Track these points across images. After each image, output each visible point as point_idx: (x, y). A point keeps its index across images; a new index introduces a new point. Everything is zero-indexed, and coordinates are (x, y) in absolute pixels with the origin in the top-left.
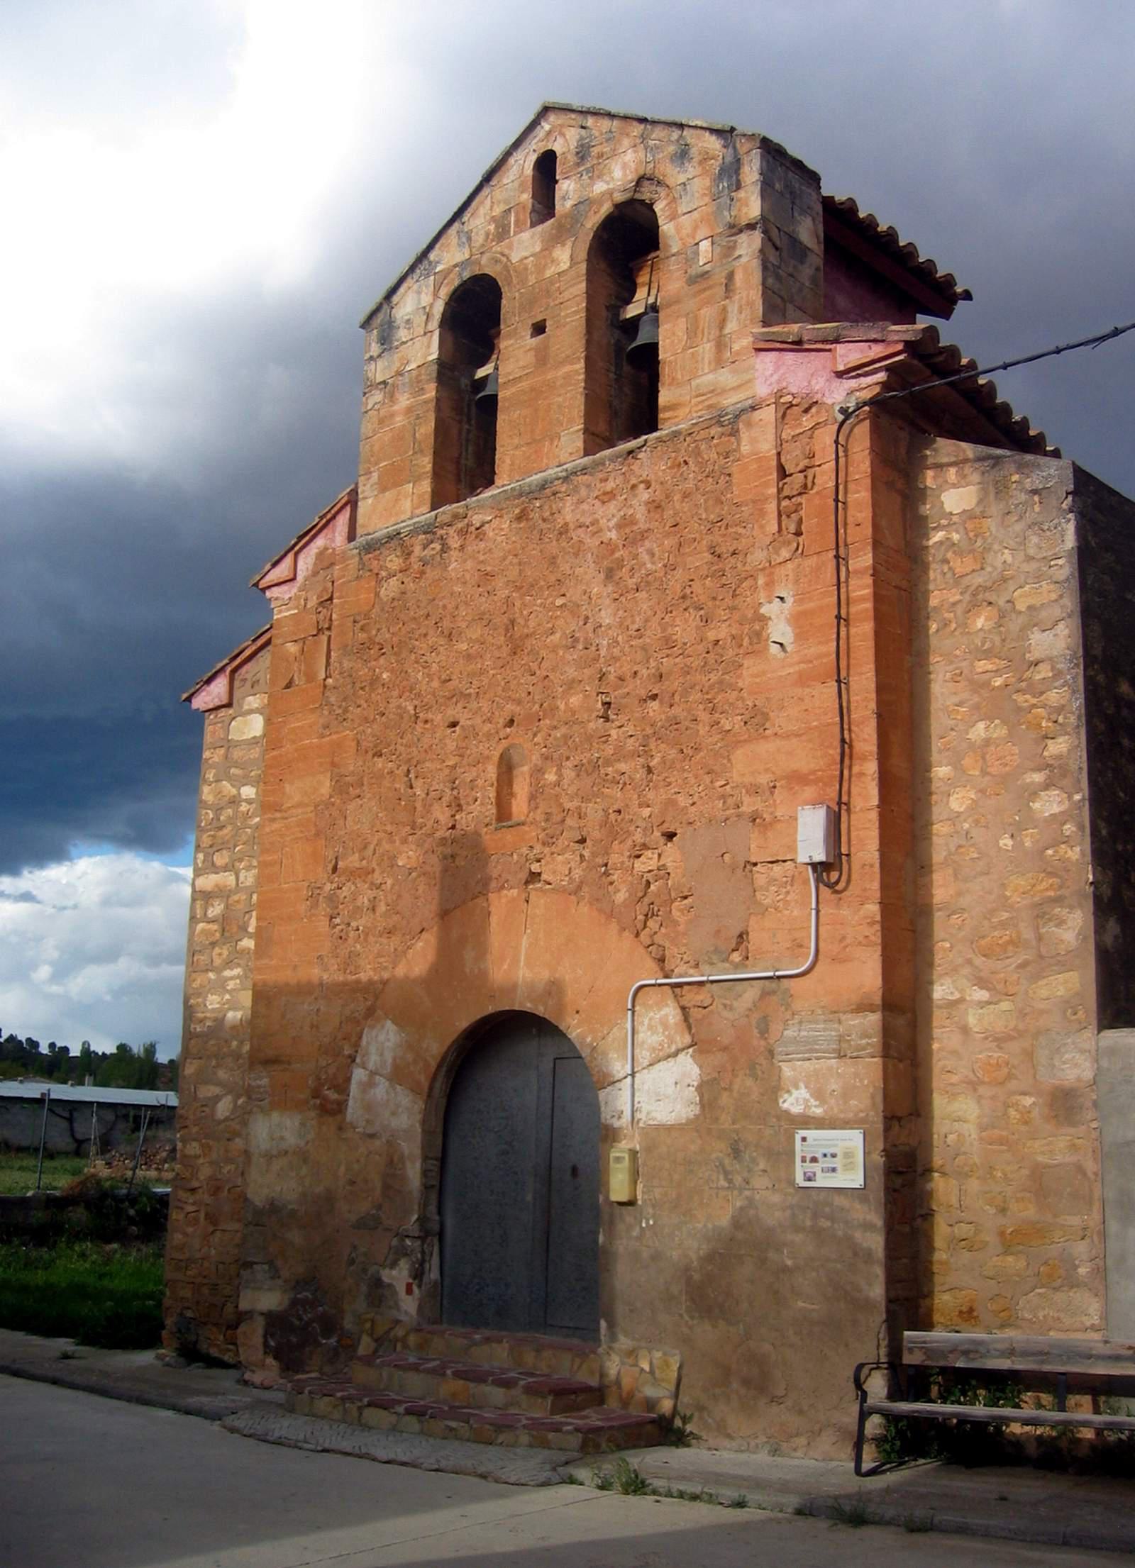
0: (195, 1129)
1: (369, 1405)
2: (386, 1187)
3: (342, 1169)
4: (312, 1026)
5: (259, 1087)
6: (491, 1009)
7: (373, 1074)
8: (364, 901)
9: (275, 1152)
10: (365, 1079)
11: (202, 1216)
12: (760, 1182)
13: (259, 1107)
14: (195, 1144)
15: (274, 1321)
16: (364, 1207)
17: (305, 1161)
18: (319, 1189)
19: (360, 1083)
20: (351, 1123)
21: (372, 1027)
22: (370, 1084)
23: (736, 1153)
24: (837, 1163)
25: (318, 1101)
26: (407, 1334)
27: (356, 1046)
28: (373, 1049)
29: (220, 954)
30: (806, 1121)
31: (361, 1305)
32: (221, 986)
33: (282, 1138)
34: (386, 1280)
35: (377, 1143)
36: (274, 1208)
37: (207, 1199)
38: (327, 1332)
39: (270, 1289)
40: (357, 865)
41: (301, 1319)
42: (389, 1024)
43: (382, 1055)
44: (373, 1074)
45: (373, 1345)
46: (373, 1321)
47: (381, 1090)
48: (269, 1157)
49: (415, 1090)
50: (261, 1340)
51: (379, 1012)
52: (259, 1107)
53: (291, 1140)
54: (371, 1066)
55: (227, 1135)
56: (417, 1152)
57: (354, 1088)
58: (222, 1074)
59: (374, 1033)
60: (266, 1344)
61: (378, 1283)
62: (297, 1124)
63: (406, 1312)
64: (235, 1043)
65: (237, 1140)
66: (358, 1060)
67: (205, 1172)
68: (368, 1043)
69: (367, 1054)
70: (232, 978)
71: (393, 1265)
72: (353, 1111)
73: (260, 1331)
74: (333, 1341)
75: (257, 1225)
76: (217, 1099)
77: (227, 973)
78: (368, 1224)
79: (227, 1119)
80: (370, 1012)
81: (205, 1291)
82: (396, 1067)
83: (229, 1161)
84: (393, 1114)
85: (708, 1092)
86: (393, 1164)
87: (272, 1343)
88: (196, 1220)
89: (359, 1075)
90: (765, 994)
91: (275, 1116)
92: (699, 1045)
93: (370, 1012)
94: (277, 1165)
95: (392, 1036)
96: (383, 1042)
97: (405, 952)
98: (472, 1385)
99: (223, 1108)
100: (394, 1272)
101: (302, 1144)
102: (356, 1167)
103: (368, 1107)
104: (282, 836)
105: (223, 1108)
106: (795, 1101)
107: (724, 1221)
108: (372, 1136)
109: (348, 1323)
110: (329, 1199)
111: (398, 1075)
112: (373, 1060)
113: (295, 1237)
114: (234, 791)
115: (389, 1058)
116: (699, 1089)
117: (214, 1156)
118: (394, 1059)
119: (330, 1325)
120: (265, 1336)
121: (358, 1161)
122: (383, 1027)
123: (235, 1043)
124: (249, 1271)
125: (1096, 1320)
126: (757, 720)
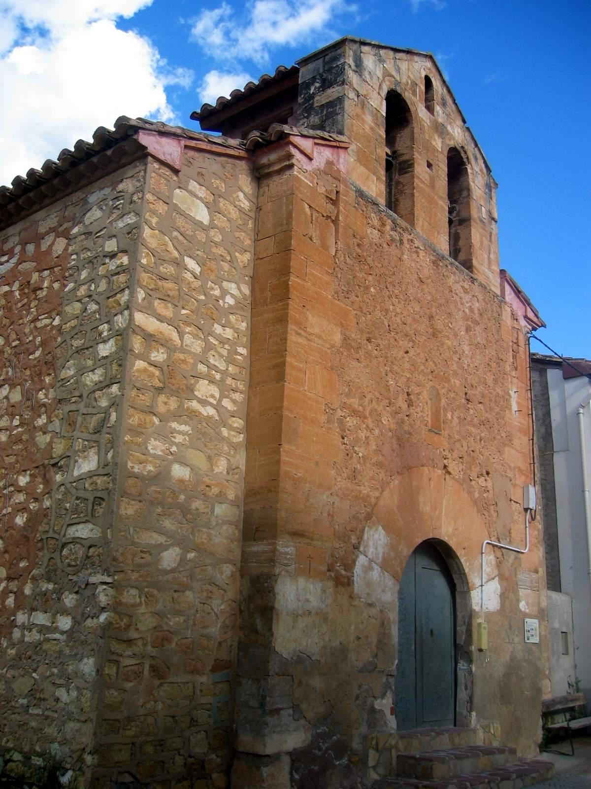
0: (134, 576)
1: (502, 780)
2: (380, 642)
3: (353, 627)
4: (329, 514)
5: (287, 553)
6: (431, 536)
7: (371, 561)
8: (362, 435)
9: (300, 612)
10: (366, 563)
11: (147, 667)
12: (516, 640)
13: (287, 571)
14: (134, 592)
15: (297, 757)
16: (367, 656)
17: (326, 620)
18: (335, 644)
19: (363, 566)
20: (358, 594)
21: (370, 528)
22: (368, 568)
23: (510, 627)
24: (533, 632)
25: (333, 574)
26: (397, 742)
27: (360, 538)
28: (371, 543)
29: (166, 403)
30: (526, 615)
31: (364, 729)
32: (165, 435)
33: (307, 600)
34: (377, 707)
35: (374, 611)
36: (300, 659)
37: (154, 652)
38: (339, 756)
39: (295, 730)
40: (356, 406)
41: (320, 749)
42: (380, 527)
43: (376, 549)
44: (371, 561)
45: (377, 755)
46: (377, 737)
47: (375, 573)
48: (296, 616)
49: (395, 577)
50: (287, 777)
51: (374, 518)
52: (287, 571)
53: (314, 603)
54: (370, 555)
55: (176, 587)
56: (397, 619)
57: (358, 570)
58: (168, 524)
59: (372, 532)
60: (292, 779)
61: (373, 710)
62: (319, 590)
63: (391, 728)
64: (182, 497)
65: (188, 593)
66: (361, 549)
67: (146, 622)
68: (368, 538)
69: (366, 546)
70: (180, 432)
71: (383, 696)
72: (358, 585)
73: (287, 768)
74: (345, 761)
75: (283, 675)
76: (163, 548)
77: (174, 425)
78: (371, 669)
79: (173, 571)
80: (369, 517)
81: (149, 749)
82: (384, 558)
83: (179, 613)
84: (383, 591)
85: (503, 596)
86: (383, 624)
87: (297, 777)
88: (138, 675)
89: (362, 560)
90: (516, 558)
91: (301, 581)
92: (501, 577)
93: (369, 517)
94: (302, 623)
95: (382, 537)
96: (376, 540)
97: (388, 483)
98: (491, 757)
99: (170, 558)
100: (384, 701)
101: (324, 606)
102: (361, 627)
103: (368, 584)
104: (306, 352)
105: (170, 558)
106: (523, 606)
107: (508, 658)
108: (371, 605)
109: (356, 745)
110: (342, 651)
111: (385, 566)
112: (371, 551)
113: (317, 682)
114: (176, 254)
115: (381, 550)
116: (501, 596)
117: (159, 606)
118: (384, 553)
119: (341, 749)
120: (291, 773)
121: (363, 623)
122: (377, 530)
123: (182, 497)
124: (276, 717)
125: (550, 690)
126: (510, 437)
